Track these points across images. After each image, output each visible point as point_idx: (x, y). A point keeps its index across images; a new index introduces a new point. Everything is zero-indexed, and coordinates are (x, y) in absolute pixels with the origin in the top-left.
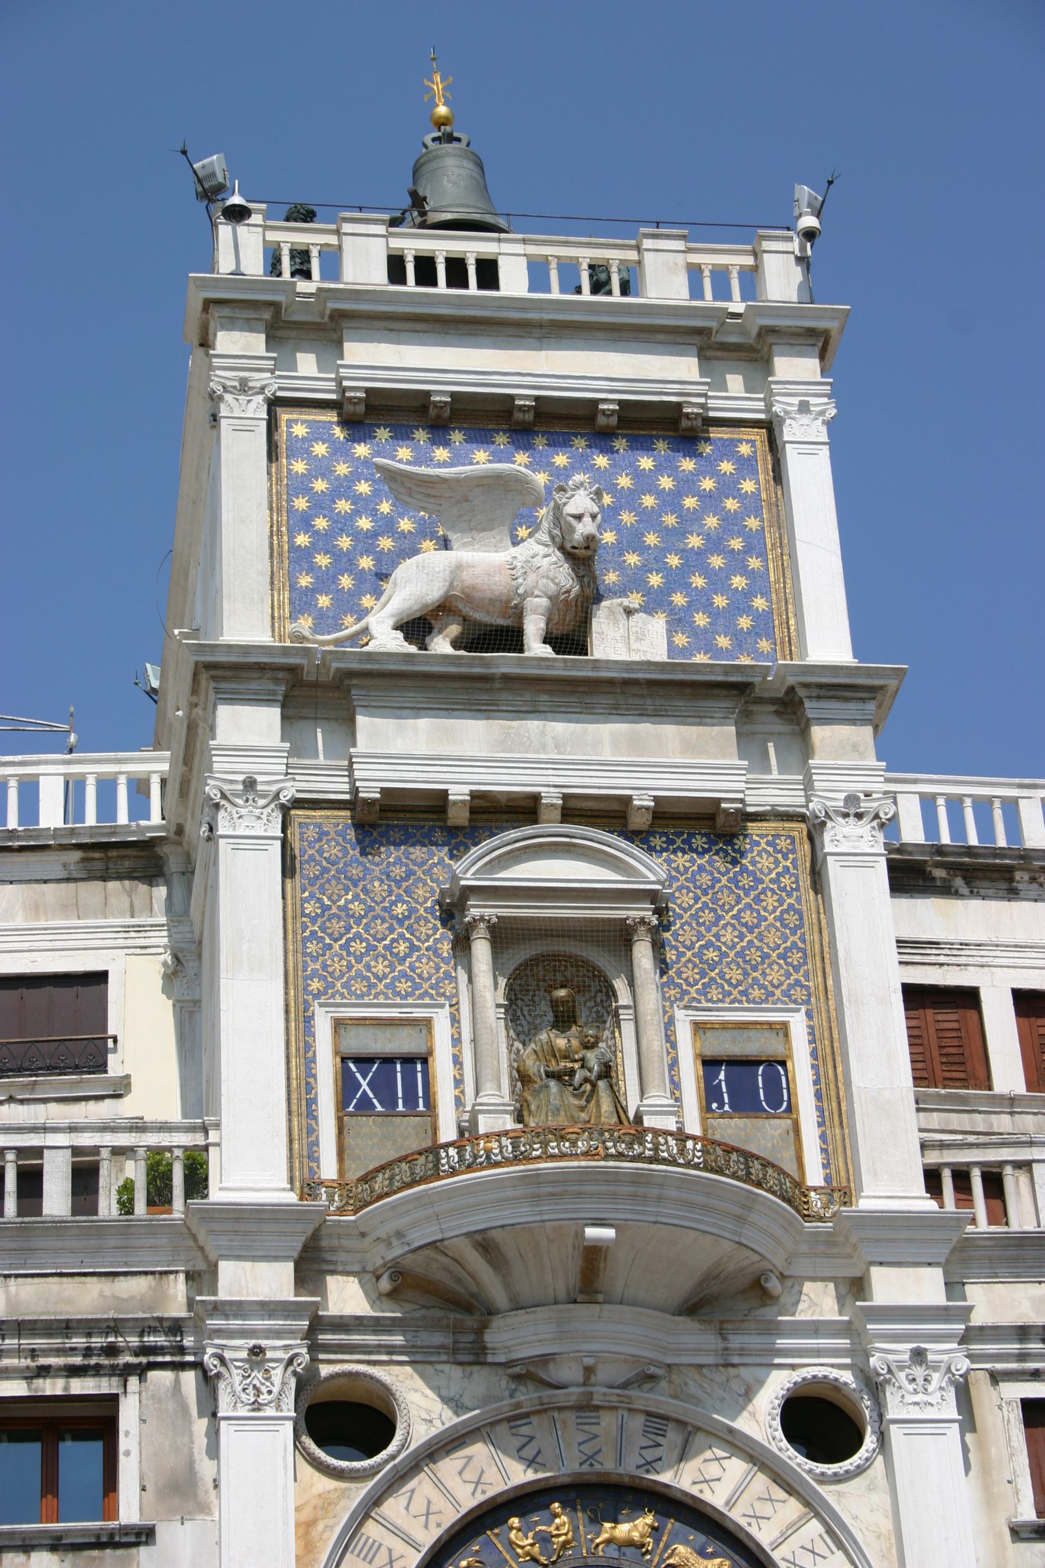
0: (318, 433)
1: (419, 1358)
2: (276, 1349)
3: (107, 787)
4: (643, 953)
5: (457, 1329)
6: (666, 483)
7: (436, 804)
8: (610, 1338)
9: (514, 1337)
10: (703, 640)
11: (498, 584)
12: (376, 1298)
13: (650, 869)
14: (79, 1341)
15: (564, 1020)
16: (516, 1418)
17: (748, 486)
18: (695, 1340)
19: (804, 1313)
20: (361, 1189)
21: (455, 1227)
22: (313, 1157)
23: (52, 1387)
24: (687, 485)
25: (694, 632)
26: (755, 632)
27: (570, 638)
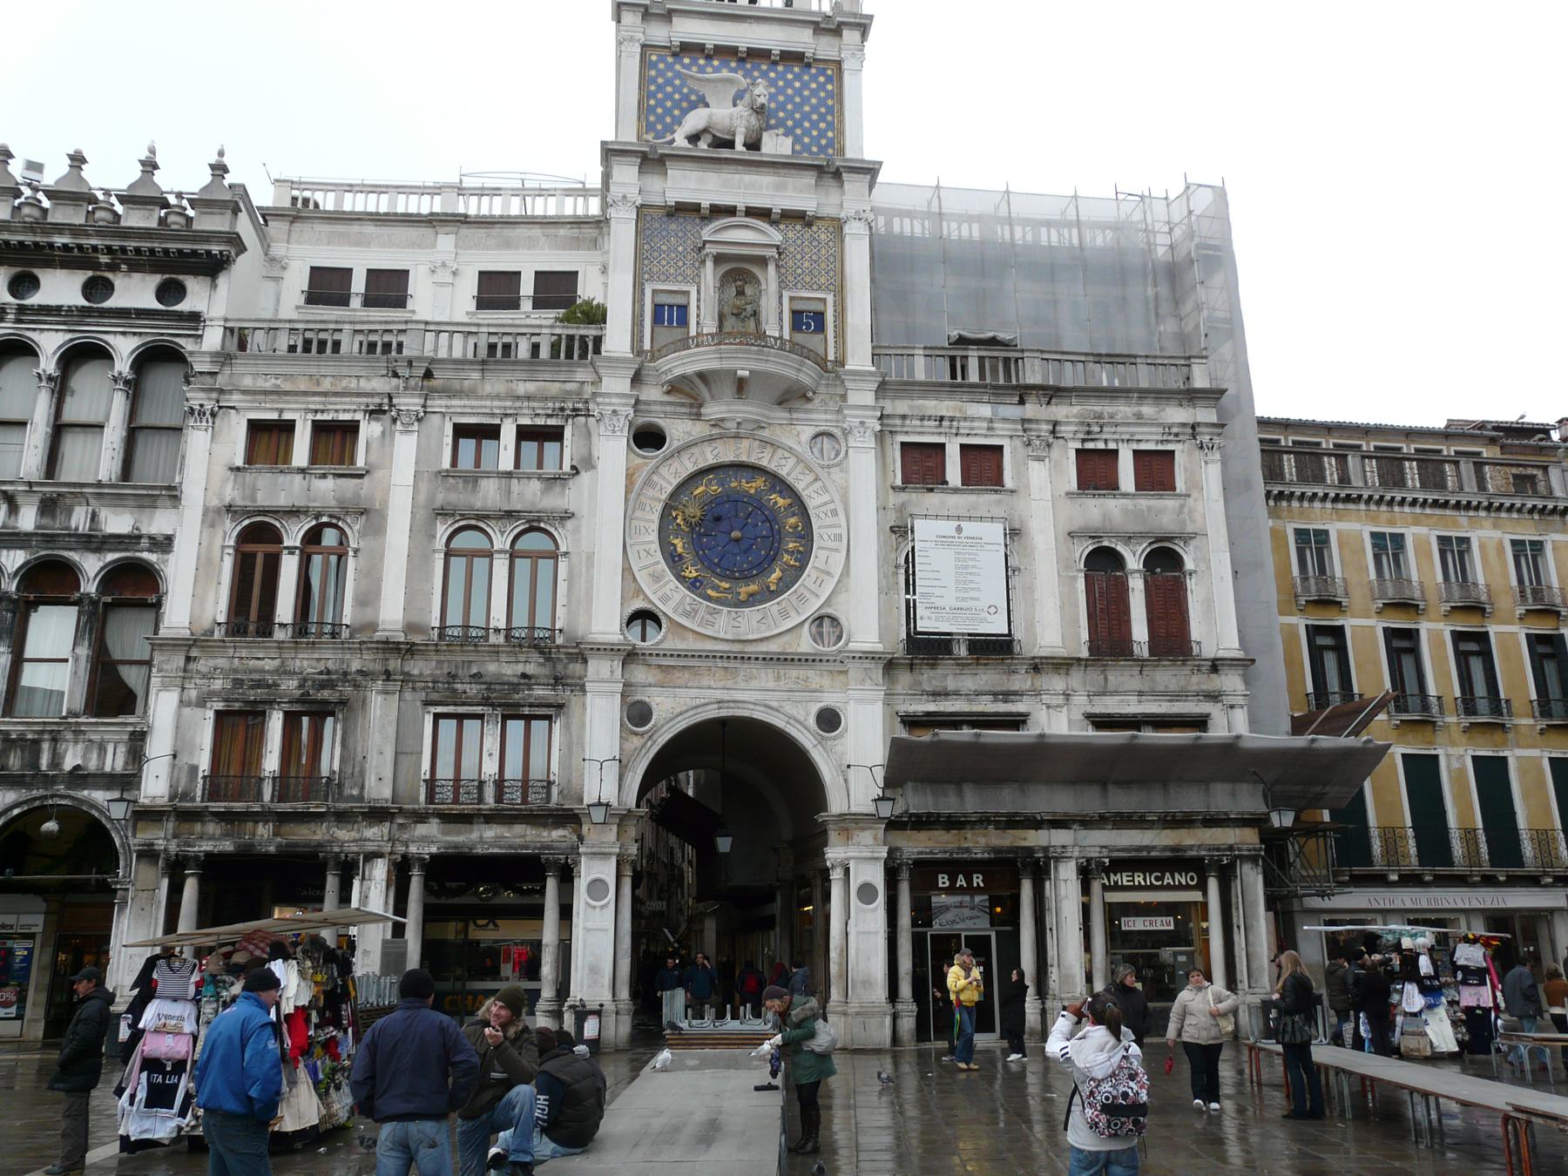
0: (662, 59)
4: (771, 269)
5: (691, 406)
6: (797, 84)
7: (695, 208)
10: (807, 148)
11: (727, 122)
13: (775, 236)
14: (550, 405)
16: (711, 439)
17: (829, 87)
21: (690, 369)
22: (642, 341)
23: (540, 421)
24: (805, 86)
26: (827, 146)
27: (753, 145)
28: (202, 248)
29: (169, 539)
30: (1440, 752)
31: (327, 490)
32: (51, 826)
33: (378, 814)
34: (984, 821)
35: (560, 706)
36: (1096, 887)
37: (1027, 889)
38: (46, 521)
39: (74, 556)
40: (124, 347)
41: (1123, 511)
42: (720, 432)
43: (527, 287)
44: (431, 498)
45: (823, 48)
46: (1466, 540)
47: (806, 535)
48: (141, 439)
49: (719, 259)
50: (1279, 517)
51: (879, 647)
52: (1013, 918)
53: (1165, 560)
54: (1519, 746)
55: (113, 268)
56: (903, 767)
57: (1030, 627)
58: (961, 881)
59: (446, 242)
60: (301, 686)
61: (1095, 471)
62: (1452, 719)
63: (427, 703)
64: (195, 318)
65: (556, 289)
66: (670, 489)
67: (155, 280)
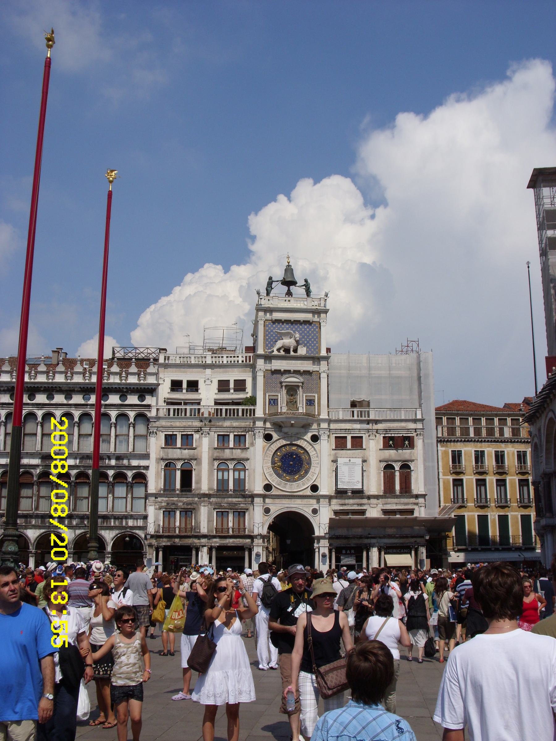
0: (269, 324)
1: (275, 431)
2: (261, 431)
3: (246, 357)
4: (300, 388)
8: (294, 430)
9: (285, 430)
12: (271, 425)
15: (292, 395)
18: (302, 430)
19: (313, 428)
20: (271, 415)
21: (279, 421)
23: (240, 433)
24: (310, 330)
25: (309, 349)
27: (295, 351)
28: (150, 387)
29: (148, 467)
30: (489, 514)
31: (186, 453)
32: (127, 539)
33: (204, 536)
34: (354, 537)
35: (248, 509)
36: (383, 553)
37: (365, 554)
38: (118, 462)
39: (125, 471)
40: (132, 414)
43: (232, 385)
44: (213, 455)
45: (316, 319)
46: (504, 451)
47: (309, 463)
48: (136, 438)
49: (286, 386)
50: (447, 447)
51: (327, 493)
52: (361, 561)
53: (406, 467)
54: (512, 511)
55: (127, 392)
56: (333, 524)
57: (368, 487)
58: (348, 552)
59: (208, 371)
60: (183, 505)
63: (214, 509)
64: (149, 406)
65: (240, 385)
66: (274, 451)
67: (138, 394)
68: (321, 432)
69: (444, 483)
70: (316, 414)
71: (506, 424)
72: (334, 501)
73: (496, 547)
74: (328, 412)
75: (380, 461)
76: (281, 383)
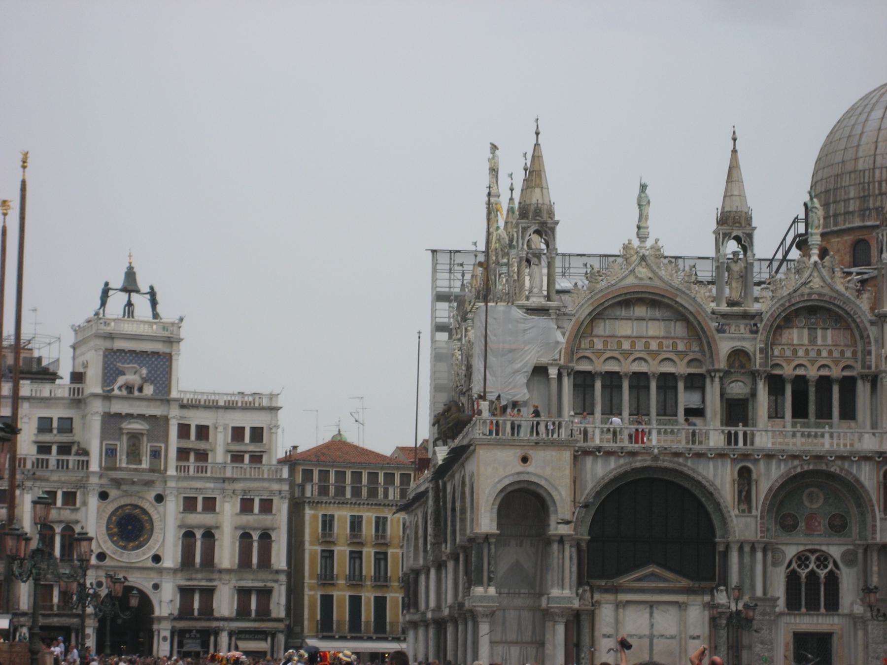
4: (145, 438)
7: (120, 414)
16: (123, 496)
27: (141, 389)
30: (363, 595)
36: (233, 639)
37: (212, 639)
41: (254, 519)
42: (127, 494)
43: (55, 424)
49: (128, 433)
50: (316, 509)
53: (266, 537)
61: (246, 506)
62: (368, 583)
65: (66, 425)
68: (167, 492)
69: (310, 554)
70: (162, 468)
71: (392, 483)
72: (179, 575)
73: (369, 635)
74: (177, 467)
75: (236, 528)
76: (121, 429)
